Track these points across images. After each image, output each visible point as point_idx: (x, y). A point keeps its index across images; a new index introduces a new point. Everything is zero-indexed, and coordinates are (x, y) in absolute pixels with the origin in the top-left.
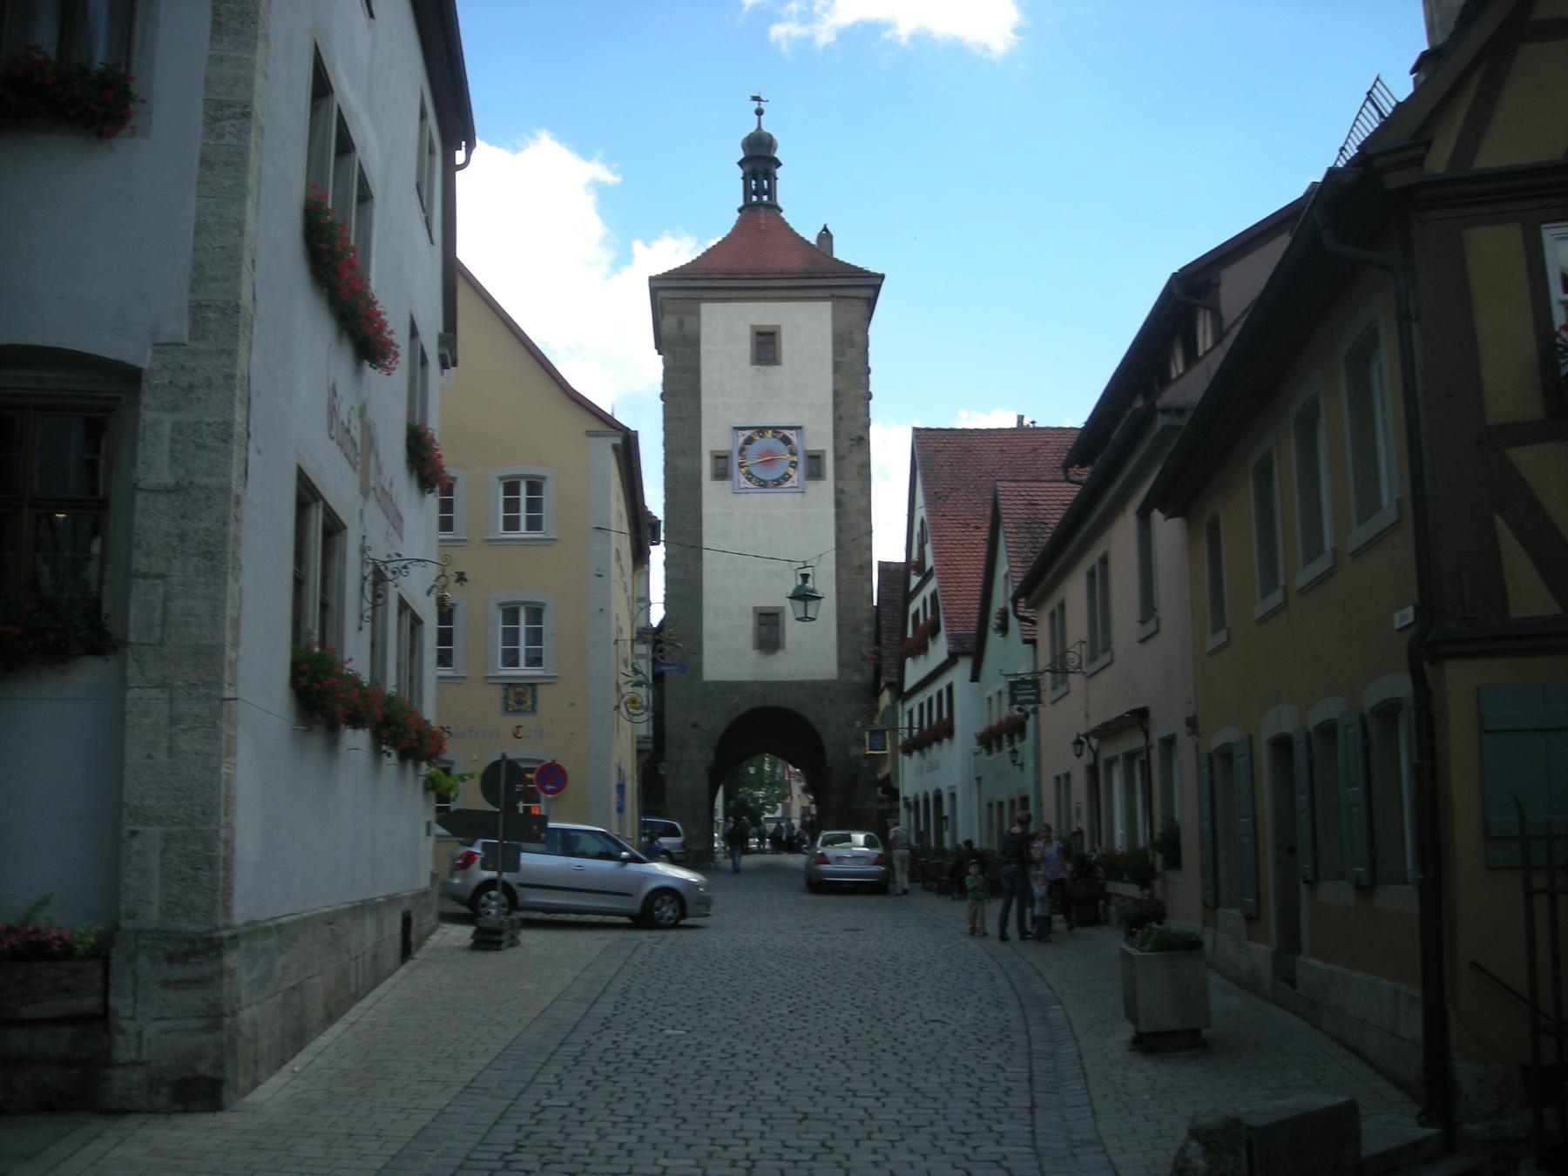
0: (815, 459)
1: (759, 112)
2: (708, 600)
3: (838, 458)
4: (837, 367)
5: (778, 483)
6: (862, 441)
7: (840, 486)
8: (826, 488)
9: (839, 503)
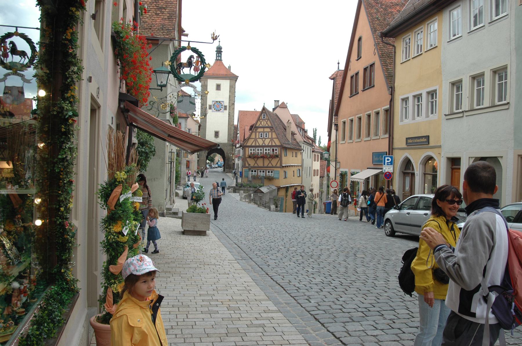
0: (226, 107)
1: (219, 42)
2: (207, 129)
3: (229, 107)
4: (230, 91)
5: (219, 111)
6: (233, 104)
7: (230, 111)
8: (227, 112)
9: (229, 114)
